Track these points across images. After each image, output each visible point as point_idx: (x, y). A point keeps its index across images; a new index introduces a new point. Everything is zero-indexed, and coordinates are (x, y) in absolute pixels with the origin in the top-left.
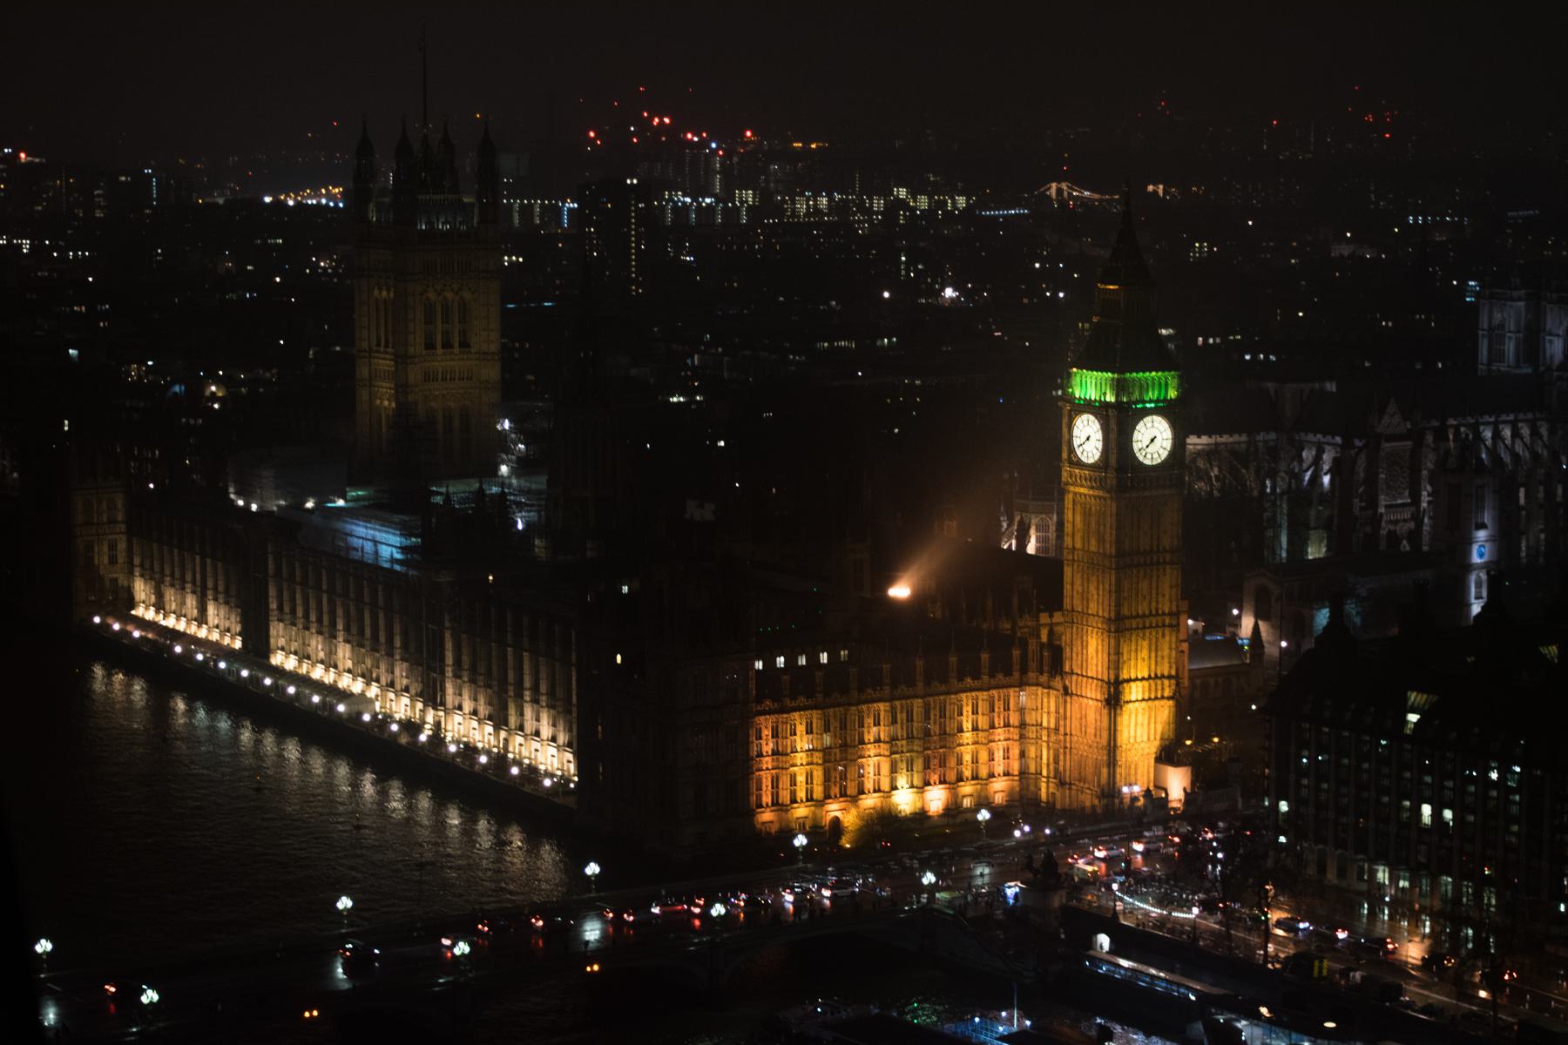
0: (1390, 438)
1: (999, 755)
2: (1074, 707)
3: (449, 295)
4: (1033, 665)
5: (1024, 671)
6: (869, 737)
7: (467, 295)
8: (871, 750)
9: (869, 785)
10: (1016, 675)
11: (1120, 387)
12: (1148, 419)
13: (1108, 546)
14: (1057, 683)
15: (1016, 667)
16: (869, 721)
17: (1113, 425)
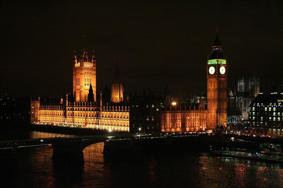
0: (232, 97)
1: (197, 123)
2: (209, 115)
3: (88, 77)
4: (201, 109)
5: (200, 110)
6: (178, 119)
7: (91, 77)
8: (178, 121)
9: (178, 127)
10: (199, 111)
11: (218, 61)
12: (222, 67)
13: (216, 87)
14: (206, 111)
15: (199, 109)
16: (178, 116)
17: (217, 67)
